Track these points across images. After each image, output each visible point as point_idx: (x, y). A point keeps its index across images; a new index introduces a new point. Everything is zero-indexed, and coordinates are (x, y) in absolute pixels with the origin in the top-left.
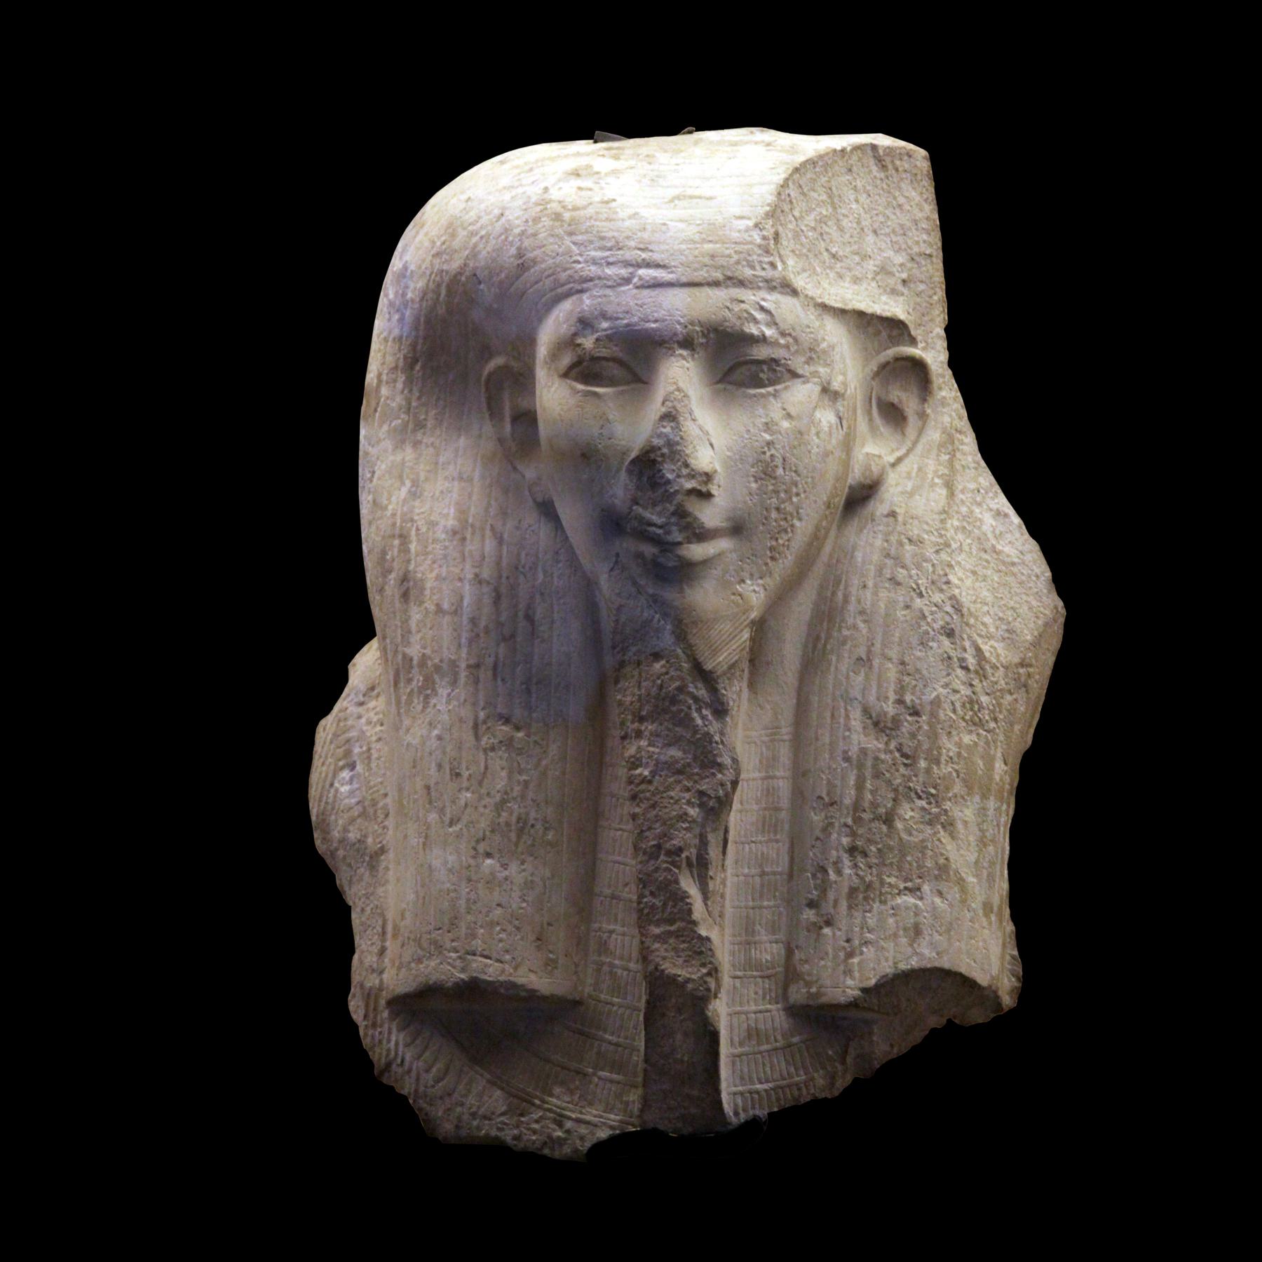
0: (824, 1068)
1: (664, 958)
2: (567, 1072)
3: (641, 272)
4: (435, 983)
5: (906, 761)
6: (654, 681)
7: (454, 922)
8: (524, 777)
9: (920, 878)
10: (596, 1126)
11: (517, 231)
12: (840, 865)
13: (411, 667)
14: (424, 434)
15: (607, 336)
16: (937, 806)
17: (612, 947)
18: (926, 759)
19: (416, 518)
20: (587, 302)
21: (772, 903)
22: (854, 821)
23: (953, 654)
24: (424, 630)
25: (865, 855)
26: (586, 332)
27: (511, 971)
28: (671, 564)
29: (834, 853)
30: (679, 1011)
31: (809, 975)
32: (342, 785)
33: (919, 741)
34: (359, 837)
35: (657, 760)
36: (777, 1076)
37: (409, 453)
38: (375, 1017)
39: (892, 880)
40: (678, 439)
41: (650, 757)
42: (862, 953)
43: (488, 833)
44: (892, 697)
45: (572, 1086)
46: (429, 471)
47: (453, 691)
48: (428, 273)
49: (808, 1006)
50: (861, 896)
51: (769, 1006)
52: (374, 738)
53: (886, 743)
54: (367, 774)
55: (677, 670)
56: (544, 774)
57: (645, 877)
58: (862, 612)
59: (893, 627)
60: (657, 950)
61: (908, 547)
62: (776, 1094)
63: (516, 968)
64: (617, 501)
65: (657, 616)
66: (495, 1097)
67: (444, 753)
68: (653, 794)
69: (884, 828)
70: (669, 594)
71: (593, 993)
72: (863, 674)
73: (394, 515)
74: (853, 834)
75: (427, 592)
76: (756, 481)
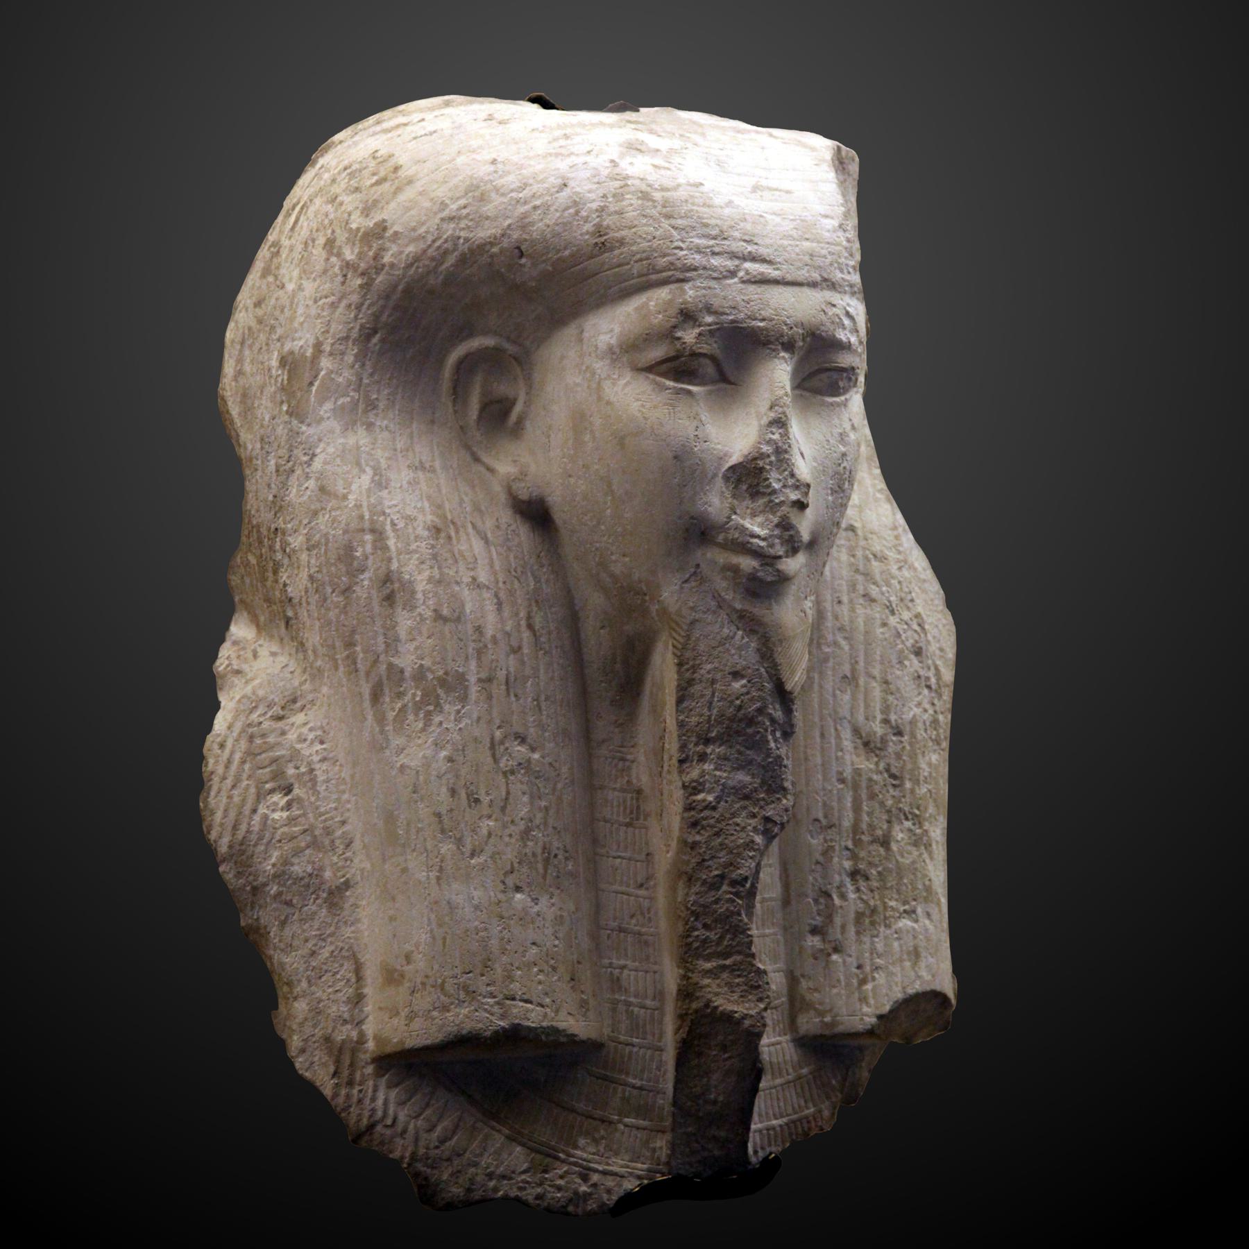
0: (828, 1098)
1: (717, 994)
2: (591, 1121)
3: (748, 265)
4: (470, 1032)
5: (894, 782)
6: (732, 702)
7: (487, 965)
8: (543, 803)
9: (915, 900)
10: (622, 1177)
11: (594, 206)
12: (844, 890)
13: (402, 680)
14: (377, 415)
15: (710, 331)
16: (921, 827)
17: (624, 984)
18: (910, 779)
19: (387, 511)
20: (690, 293)
21: (771, 931)
22: (855, 844)
23: (922, 673)
24: (420, 639)
25: (867, 878)
26: (686, 325)
27: (553, 1015)
28: (769, 579)
29: (837, 878)
30: (724, 1048)
31: (820, 1004)
32: (273, 811)
33: (904, 761)
34: (309, 869)
35: (723, 785)
36: (790, 1110)
37: (360, 437)
38: (352, 1074)
39: (892, 903)
40: (786, 447)
41: (717, 782)
42: (874, 979)
43: (516, 865)
44: (879, 717)
45: (597, 1136)
46: (389, 458)
47: (463, 707)
48: (430, 238)
49: (821, 1036)
50: (867, 921)
51: (778, 1038)
52: (316, 758)
53: (877, 764)
54: (313, 799)
55: (759, 689)
56: (560, 799)
57: (700, 910)
58: (841, 629)
59: (874, 645)
60: (708, 986)
61: (875, 563)
62: (789, 1128)
63: (557, 1011)
64: (710, 509)
65: (740, 633)
66: (516, 1153)
67: (457, 776)
68: (718, 821)
69: (882, 850)
70: (758, 610)
71: (612, 1034)
72: (849, 692)
73: (358, 506)
74: (854, 857)
75: (419, 596)
76: (832, 494)
